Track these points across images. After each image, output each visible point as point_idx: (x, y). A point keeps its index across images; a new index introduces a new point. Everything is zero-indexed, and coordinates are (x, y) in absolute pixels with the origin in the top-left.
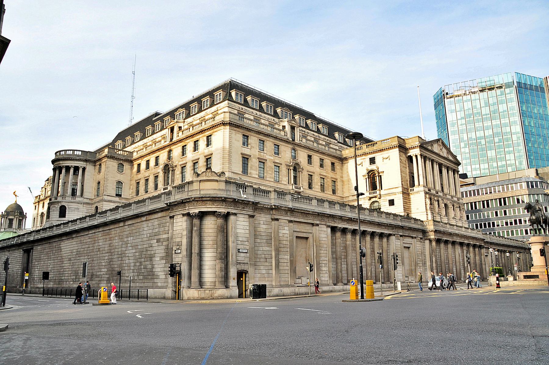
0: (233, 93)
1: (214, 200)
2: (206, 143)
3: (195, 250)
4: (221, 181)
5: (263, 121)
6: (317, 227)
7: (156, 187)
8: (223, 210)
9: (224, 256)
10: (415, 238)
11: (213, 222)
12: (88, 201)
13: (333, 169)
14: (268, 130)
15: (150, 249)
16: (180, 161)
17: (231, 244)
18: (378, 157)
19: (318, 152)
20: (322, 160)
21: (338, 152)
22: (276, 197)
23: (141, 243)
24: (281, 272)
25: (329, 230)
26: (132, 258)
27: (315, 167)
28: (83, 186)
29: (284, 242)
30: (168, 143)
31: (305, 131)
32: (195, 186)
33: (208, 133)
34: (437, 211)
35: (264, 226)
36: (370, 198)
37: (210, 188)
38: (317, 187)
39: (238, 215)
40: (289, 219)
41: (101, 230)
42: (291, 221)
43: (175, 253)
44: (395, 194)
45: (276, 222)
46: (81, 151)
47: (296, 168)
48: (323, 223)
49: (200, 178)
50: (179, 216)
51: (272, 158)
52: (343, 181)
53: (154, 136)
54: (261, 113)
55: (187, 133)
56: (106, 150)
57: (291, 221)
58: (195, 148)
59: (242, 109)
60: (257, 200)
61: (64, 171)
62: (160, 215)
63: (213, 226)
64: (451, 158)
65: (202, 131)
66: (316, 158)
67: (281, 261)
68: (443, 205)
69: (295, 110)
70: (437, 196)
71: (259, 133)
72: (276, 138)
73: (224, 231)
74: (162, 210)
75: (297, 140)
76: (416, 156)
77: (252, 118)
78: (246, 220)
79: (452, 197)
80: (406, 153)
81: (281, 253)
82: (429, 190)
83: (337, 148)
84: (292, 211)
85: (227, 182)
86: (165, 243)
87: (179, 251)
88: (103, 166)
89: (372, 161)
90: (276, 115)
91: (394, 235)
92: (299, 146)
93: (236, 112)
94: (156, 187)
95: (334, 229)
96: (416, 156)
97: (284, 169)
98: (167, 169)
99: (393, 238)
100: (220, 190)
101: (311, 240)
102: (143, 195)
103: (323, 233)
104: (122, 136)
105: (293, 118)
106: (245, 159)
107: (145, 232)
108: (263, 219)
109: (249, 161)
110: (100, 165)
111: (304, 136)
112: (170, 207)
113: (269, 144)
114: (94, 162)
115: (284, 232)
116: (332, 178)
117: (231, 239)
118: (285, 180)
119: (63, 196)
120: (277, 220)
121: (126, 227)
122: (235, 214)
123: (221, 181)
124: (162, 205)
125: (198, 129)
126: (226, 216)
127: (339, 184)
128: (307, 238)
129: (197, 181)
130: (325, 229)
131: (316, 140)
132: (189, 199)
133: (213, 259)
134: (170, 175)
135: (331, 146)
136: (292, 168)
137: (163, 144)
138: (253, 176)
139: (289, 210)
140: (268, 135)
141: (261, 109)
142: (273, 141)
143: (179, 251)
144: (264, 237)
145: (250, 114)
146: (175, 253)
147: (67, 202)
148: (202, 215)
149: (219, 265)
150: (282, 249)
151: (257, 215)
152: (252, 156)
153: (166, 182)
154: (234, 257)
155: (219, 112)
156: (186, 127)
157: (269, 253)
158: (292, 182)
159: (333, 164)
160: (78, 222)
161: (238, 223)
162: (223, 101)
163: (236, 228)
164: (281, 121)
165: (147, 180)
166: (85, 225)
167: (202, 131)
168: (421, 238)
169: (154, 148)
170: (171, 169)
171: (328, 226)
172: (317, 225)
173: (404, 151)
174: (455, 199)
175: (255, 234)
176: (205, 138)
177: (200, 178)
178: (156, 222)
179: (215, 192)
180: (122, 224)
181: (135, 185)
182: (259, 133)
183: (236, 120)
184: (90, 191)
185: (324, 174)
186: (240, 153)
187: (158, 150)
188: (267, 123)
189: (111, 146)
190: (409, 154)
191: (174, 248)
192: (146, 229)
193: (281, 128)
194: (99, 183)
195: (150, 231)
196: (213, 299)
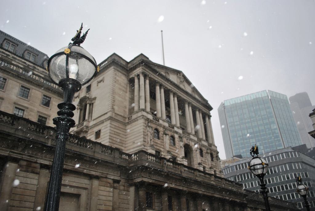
10: (97, 178)
31: (9, 55)
44: (102, 122)
64: (197, 97)
68: (182, 144)
79: (200, 140)
91: (15, 160)
96: (138, 76)
116: (38, 112)
168: (115, 181)
173: (125, 73)
174: (205, 144)
185: (26, 105)
190: (131, 77)
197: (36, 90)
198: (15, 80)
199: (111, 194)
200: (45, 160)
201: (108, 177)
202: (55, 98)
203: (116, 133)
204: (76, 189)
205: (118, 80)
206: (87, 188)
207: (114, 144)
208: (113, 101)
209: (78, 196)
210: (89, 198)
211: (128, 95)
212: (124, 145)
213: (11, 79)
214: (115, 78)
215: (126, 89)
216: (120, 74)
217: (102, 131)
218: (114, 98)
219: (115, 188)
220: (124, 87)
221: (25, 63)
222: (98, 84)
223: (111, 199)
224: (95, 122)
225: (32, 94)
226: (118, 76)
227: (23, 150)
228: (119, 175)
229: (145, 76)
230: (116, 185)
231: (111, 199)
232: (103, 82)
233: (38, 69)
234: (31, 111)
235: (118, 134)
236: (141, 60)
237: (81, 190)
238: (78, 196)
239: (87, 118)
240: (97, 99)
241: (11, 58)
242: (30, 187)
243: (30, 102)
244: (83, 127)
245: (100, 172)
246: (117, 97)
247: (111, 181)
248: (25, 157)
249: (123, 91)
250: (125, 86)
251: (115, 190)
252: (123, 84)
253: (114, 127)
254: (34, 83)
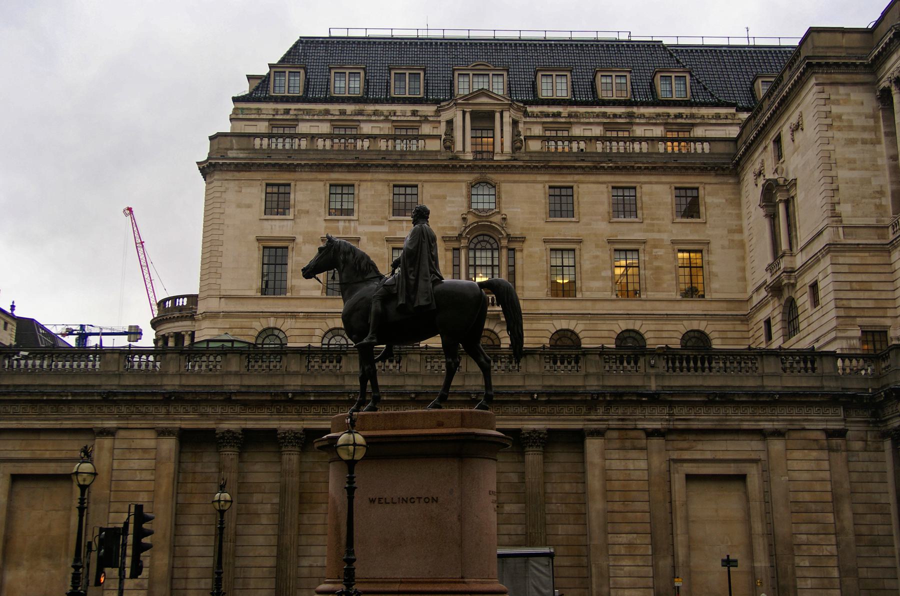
6: (107, 442)
25: (169, 445)
31: (558, 115)
44: (816, 259)
46: (187, 296)
51: (384, 229)
91: (598, 433)
95: (190, 440)
99: (593, 446)
116: (673, 242)
130: (151, 443)
138: (303, 294)
152: (299, 239)
168: (831, 434)
171: (162, 433)
186: (253, 238)
190: (884, 84)
197: (650, 183)
198: (592, 178)
199: (825, 465)
200: (655, 420)
201: (807, 427)
202: (710, 184)
203: (855, 286)
204: (732, 465)
205: (839, 117)
206: (760, 460)
207: (856, 317)
208: (830, 193)
209: (742, 478)
210: (766, 480)
212: (890, 313)
213: (583, 182)
214: (828, 114)
215: (875, 129)
216: (842, 90)
217: (821, 285)
218: (833, 179)
219: (830, 449)
220: (864, 129)
221: (604, 115)
222: (792, 135)
223: (827, 475)
225: (645, 199)
226: (837, 103)
227: (607, 412)
228: (842, 417)
230: (835, 442)
231: (827, 475)
232: (802, 129)
233: (642, 116)
234: (655, 247)
235: (864, 287)
236: (890, 30)
237: (748, 465)
238: (742, 478)
239: (784, 246)
240: (798, 182)
241: (568, 120)
242: (636, 475)
243: (646, 222)
244: (779, 273)
245: (783, 420)
246: (843, 174)
247: (821, 436)
248: (614, 424)
249: (864, 142)
250: (871, 122)
251: (832, 453)
252: (859, 122)
253: (845, 269)
254: (640, 168)
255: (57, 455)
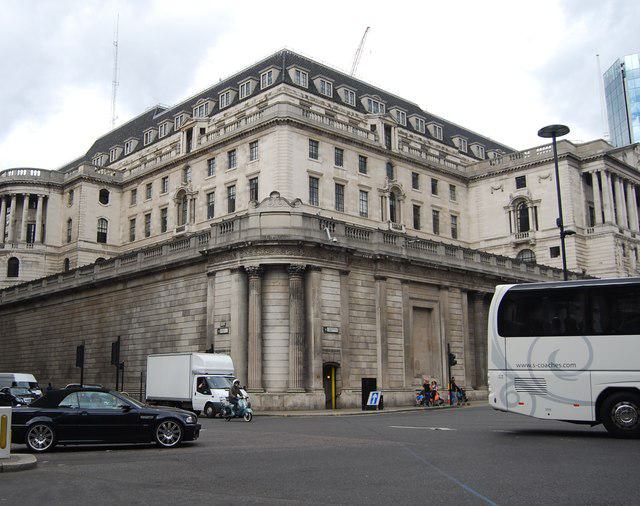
0: (292, 72)
1: (284, 244)
2: (248, 154)
3: (255, 329)
4: (295, 214)
5: (339, 117)
6: (446, 293)
7: (164, 228)
8: (298, 261)
9: (303, 338)
11: (281, 282)
12: (53, 250)
13: (453, 197)
14: (350, 132)
15: (172, 327)
16: (203, 185)
17: (313, 319)
18: (531, 176)
19: (428, 167)
20: (434, 183)
21: (461, 169)
22: (381, 240)
23: (156, 318)
24: (391, 365)
25: (465, 297)
26: (141, 341)
27: (424, 194)
28: (43, 226)
29: (395, 316)
30: (183, 153)
32: (253, 222)
33: (251, 138)
34: (634, 267)
35: (364, 290)
36: (517, 245)
37: (276, 225)
38: (427, 226)
39: (324, 271)
40: (402, 277)
41: (83, 296)
42: (404, 282)
43: (219, 333)
45: (382, 283)
47: (395, 194)
48: (456, 285)
49: (259, 210)
50: (225, 273)
51: (356, 178)
52: (469, 218)
53: (159, 145)
54: (336, 104)
55: (213, 139)
56: (81, 168)
57: (404, 282)
58: (231, 163)
59: (307, 97)
60: (353, 245)
61: (13, 202)
62: (188, 271)
63: (281, 289)
65: (242, 135)
66: (425, 179)
67: (391, 347)
69: (391, 101)
70: (634, 242)
71: (335, 136)
72: (362, 145)
73: (301, 296)
74: (192, 263)
75: (395, 148)
76: (598, 173)
77: (323, 112)
78: (335, 278)
80: (579, 168)
81: (391, 334)
82: (621, 231)
83: (458, 161)
84: (406, 264)
85: (305, 216)
86: (197, 318)
87: (226, 330)
88: (76, 194)
89: (521, 183)
90: (359, 107)
92: (400, 158)
93: (297, 102)
94: (164, 228)
96: (598, 173)
97: (374, 196)
98: (182, 197)
100: (294, 228)
101: (436, 312)
102: (141, 242)
103: (455, 301)
104: (103, 145)
105: (387, 111)
106: (314, 181)
107: (162, 300)
108: (361, 277)
109: (320, 182)
110: (71, 192)
111: (405, 142)
112: (208, 257)
113: (351, 156)
114: (61, 188)
115: (394, 298)
117: (313, 311)
118: (375, 213)
119: (14, 242)
120: (384, 279)
121: (128, 291)
122: (319, 269)
123: (295, 214)
124: (194, 253)
125: (232, 131)
126: (304, 273)
127: (462, 222)
128: (429, 310)
129: (255, 214)
131: (425, 149)
132: (243, 243)
133: (285, 343)
134: (188, 207)
135: (448, 158)
136: (387, 194)
137: (174, 156)
138: (327, 207)
139: (403, 263)
140: (349, 141)
141: (336, 99)
142: (357, 150)
143: (226, 330)
144: (363, 308)
145: (319, 106)
146: (219, 333)
147: (19, 251)
148: (265, 271)
149: (294, 353)
150: (392, 328)
151: (352, 270)
153: (182, 219)
154: (318, 340)
155: (270, 103)
156: (214, 128)
157: (372, 334)
158: (389, 218)
159: (452, 188)
160: (44, 283)
161: (324, 283)
162: (277, 84)
163: (320, 292)
164: (368, 117)
165: (148, 216)
166: (56, 288)
167: (242, 135)
169: (159, 163)
170: (189, 197)
171: (463, 291)
172: (447, 288)
175: (350, 303)
176: (247, 146)
177: (259, 210)
178: (181, 284)
179: (286, 232)
180: (120, 287)
181: (128, 223)
182: (335, 136)
183: (297, 114)
184: (55, 235)
187: (168, 167)
188: (347, 120)
189: (87, 159)
190: (585, 171)
191: (217, 326)
192: (162, 294)
193: (369, 128)
194: (70, 221)
195: (172, 298)
196: (285, 410)
211: (582, 198)
224: (545, 235)
229: (607, 172)
255: (427, 298)
